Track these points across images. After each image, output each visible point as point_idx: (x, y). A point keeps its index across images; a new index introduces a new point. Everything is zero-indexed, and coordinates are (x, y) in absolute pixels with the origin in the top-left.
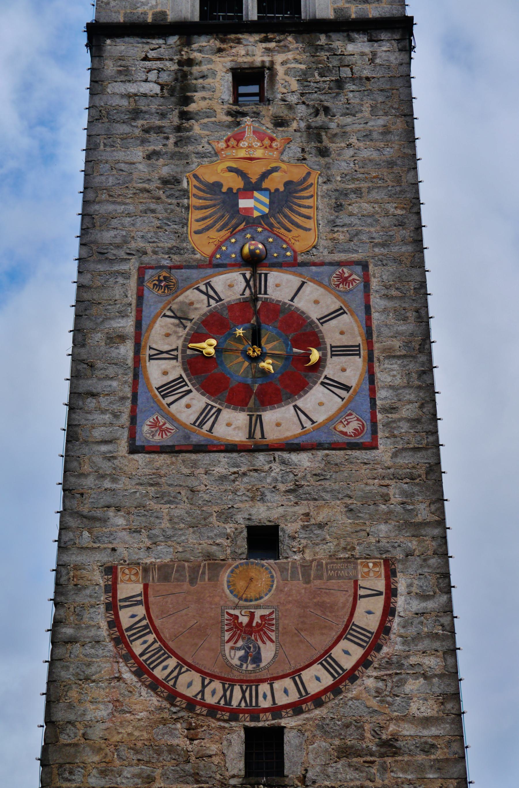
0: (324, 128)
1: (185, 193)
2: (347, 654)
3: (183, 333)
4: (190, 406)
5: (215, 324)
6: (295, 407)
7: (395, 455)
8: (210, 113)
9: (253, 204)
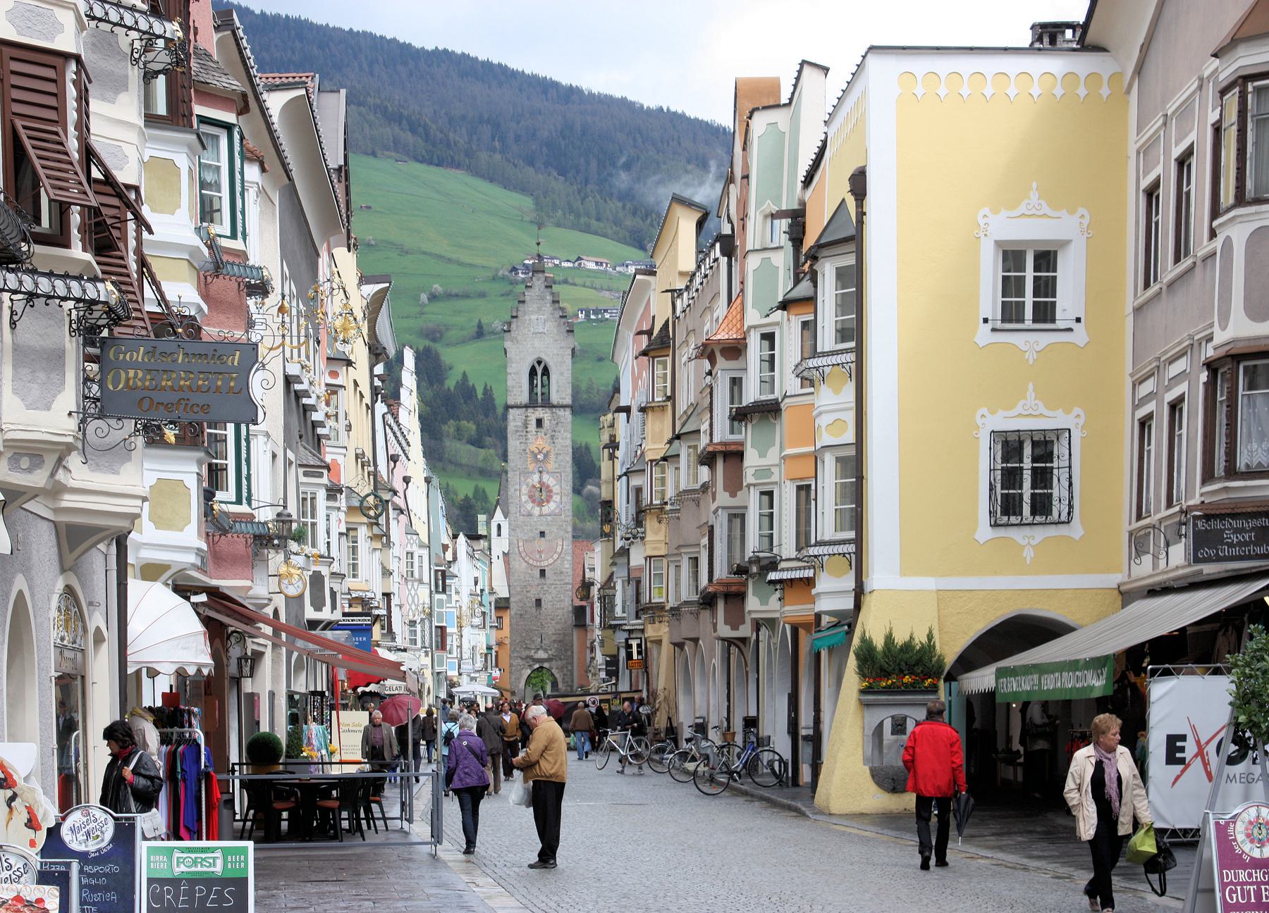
2: (556, 556)
4: (529, 506)
9: (540, 457)
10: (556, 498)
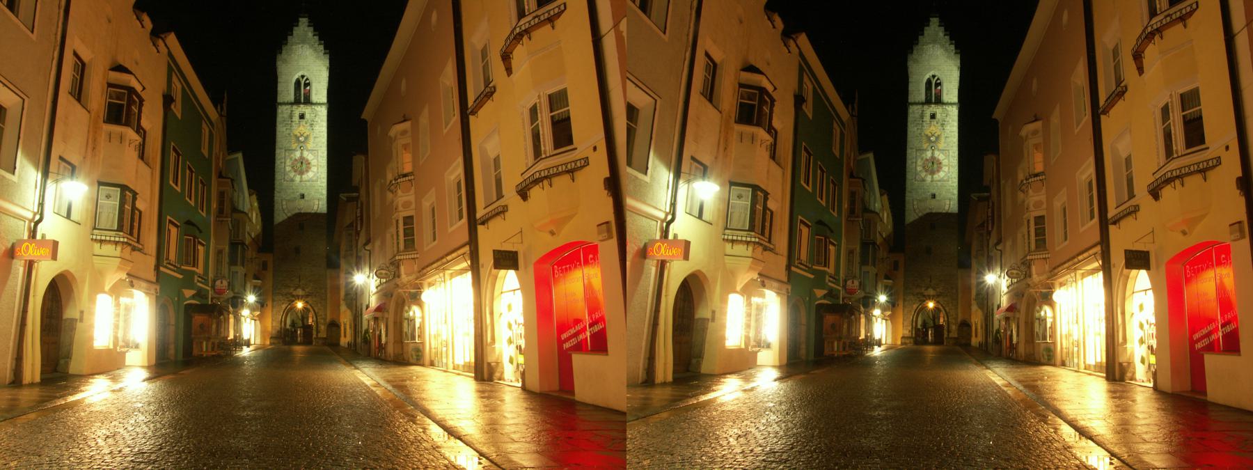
10: (946, 169)
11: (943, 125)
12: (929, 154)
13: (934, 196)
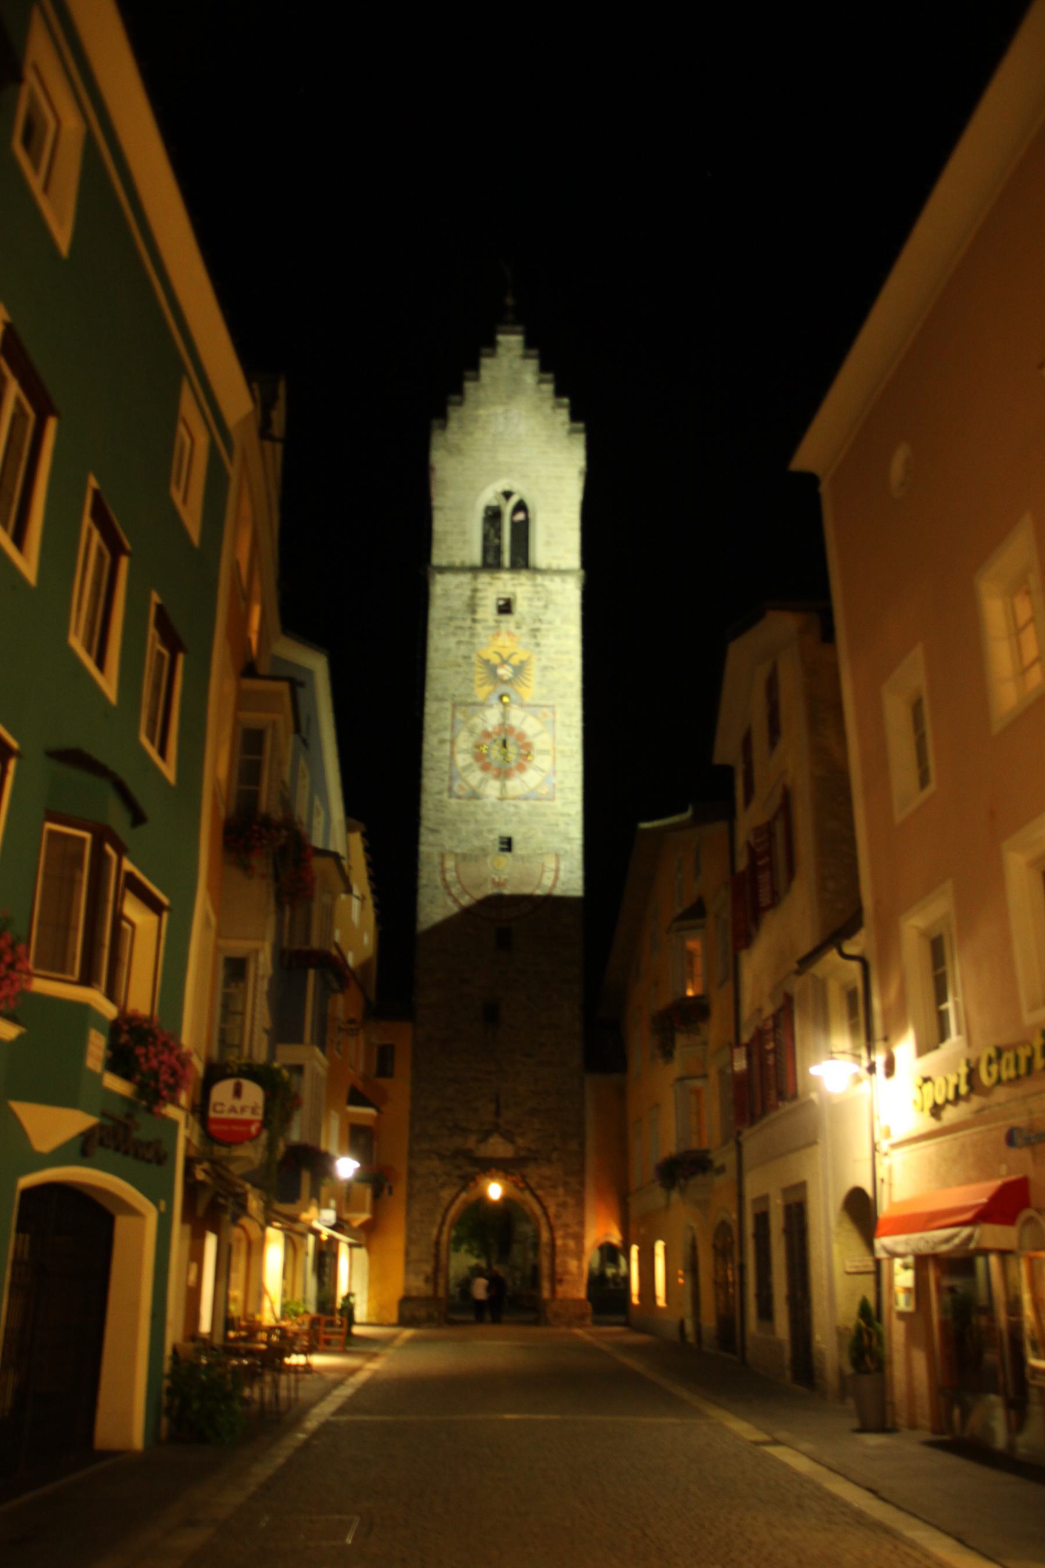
0: (537, 630)
1: (472, 664)
3: (472, 740)
4: (475, 777)
5: (487, 734)
6: (523, 781)
7: (564, 804)
8: (485, 621)
9: (505, 672)
10: (541, 761)
11: (534, 632)
12: (492, 718)
13: (507, 844)
